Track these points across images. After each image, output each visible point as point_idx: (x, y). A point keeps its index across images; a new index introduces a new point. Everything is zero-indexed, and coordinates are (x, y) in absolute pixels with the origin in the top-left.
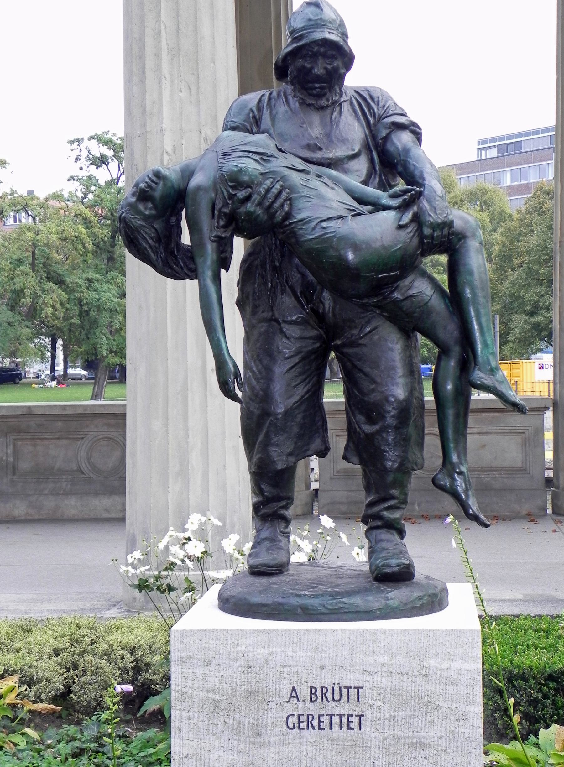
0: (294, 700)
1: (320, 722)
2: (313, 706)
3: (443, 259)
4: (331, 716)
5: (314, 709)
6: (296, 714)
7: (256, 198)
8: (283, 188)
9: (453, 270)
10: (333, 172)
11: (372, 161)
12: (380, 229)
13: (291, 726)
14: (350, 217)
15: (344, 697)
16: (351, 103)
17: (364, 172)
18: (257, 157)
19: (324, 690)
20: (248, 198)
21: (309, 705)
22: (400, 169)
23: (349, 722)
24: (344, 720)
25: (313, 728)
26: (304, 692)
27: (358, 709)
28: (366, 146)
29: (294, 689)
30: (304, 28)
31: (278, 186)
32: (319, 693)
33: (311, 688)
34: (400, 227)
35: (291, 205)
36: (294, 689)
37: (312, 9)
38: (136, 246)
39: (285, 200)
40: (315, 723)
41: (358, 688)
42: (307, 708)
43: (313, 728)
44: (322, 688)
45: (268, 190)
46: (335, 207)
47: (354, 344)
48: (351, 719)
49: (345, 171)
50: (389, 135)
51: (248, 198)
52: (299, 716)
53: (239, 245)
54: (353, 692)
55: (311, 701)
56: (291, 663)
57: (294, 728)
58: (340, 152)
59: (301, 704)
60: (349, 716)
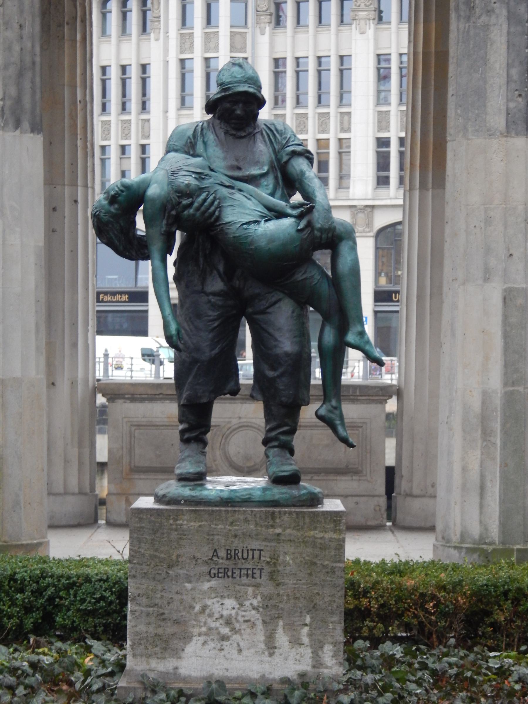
0: (215, 559)
1: (233, 573)
2: (227, 562)
3: (328, 252)
4: (241, 569)
6: (217, 567)
7: (196, 205)
8: (215, 199)
10: (250, 187)
11: (276, 178)
13: (213, 576)
14: (263, 222)
15: (250, 556)
16: (262, 134)
17: (271, 186)
19: (237, 552)
20: (190, 205)
22: (297, 185)
23: (253, 573)
24: (250, 572)
25: (228, 577)
27: (259, 564)
28: (272, 167)
29: (215, 550)
30: (230, 83)
31: (211, 198)
32: (233, 554)
33: (228, 550)
35: (220, 211)
36: (215, 550)
37: (236, 68)
38: (163, 289)
39: (216, 208)
40: (230, 574)
41: (260, 551)
42: (223, 563)
43: (228, 577)
44: (235, 550)
45: (205, 200)
46: (251, 216)
47: (263, 312)
48: (255, 571)
49: (257, 186)
50: (289, 159)
51: (190, 205)
52: (218, 569)
54: (257, 553)
55: (227, 559)
56: (215, 533)
57: (215, 576)
58: (255, 171)
60: (253, 569)
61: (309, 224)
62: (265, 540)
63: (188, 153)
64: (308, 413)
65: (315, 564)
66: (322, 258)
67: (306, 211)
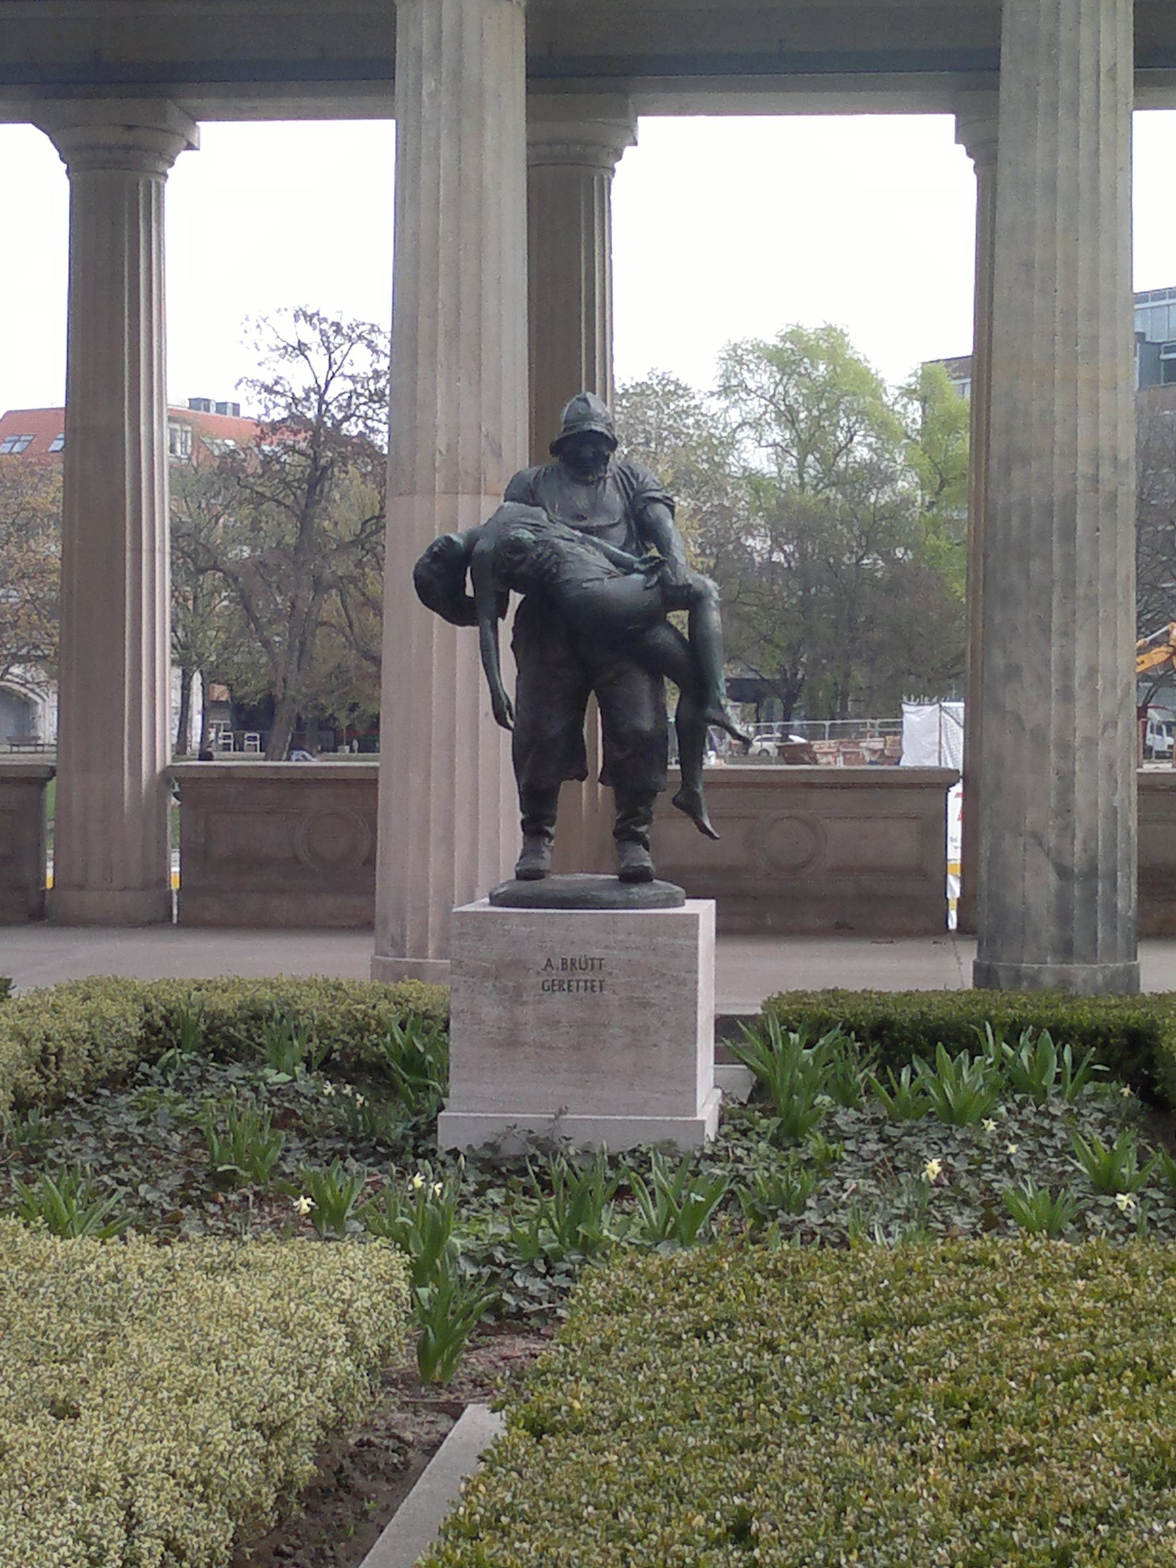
0: (549, 969)
2: (564, 973)
3: (684, 614)
4: (578, 981)
5: (564, 975)
9: (694, 622)
10: (596, 539)
11: (629, 528)
12: (631, 587)
18: (531, 528)
20: (521, 563)
21: (561, 972)
23: (593, 987)
24: (589, 984)
26: (557, 962)
28: (626, 515)
30: (574, 421)
34: (646, 588)
40: (565, 986)
41: (602, 959)
42: (557, 974)
49: (606, 538)
51: (521, 563)
53: (516, 599)
59: (554, 972)
61: (662, 582)
62: (607, 947)
63: (526, 503)
64: (662, 802)
65: (664, 975)
66: (679, 618)
67: (655, 567)
